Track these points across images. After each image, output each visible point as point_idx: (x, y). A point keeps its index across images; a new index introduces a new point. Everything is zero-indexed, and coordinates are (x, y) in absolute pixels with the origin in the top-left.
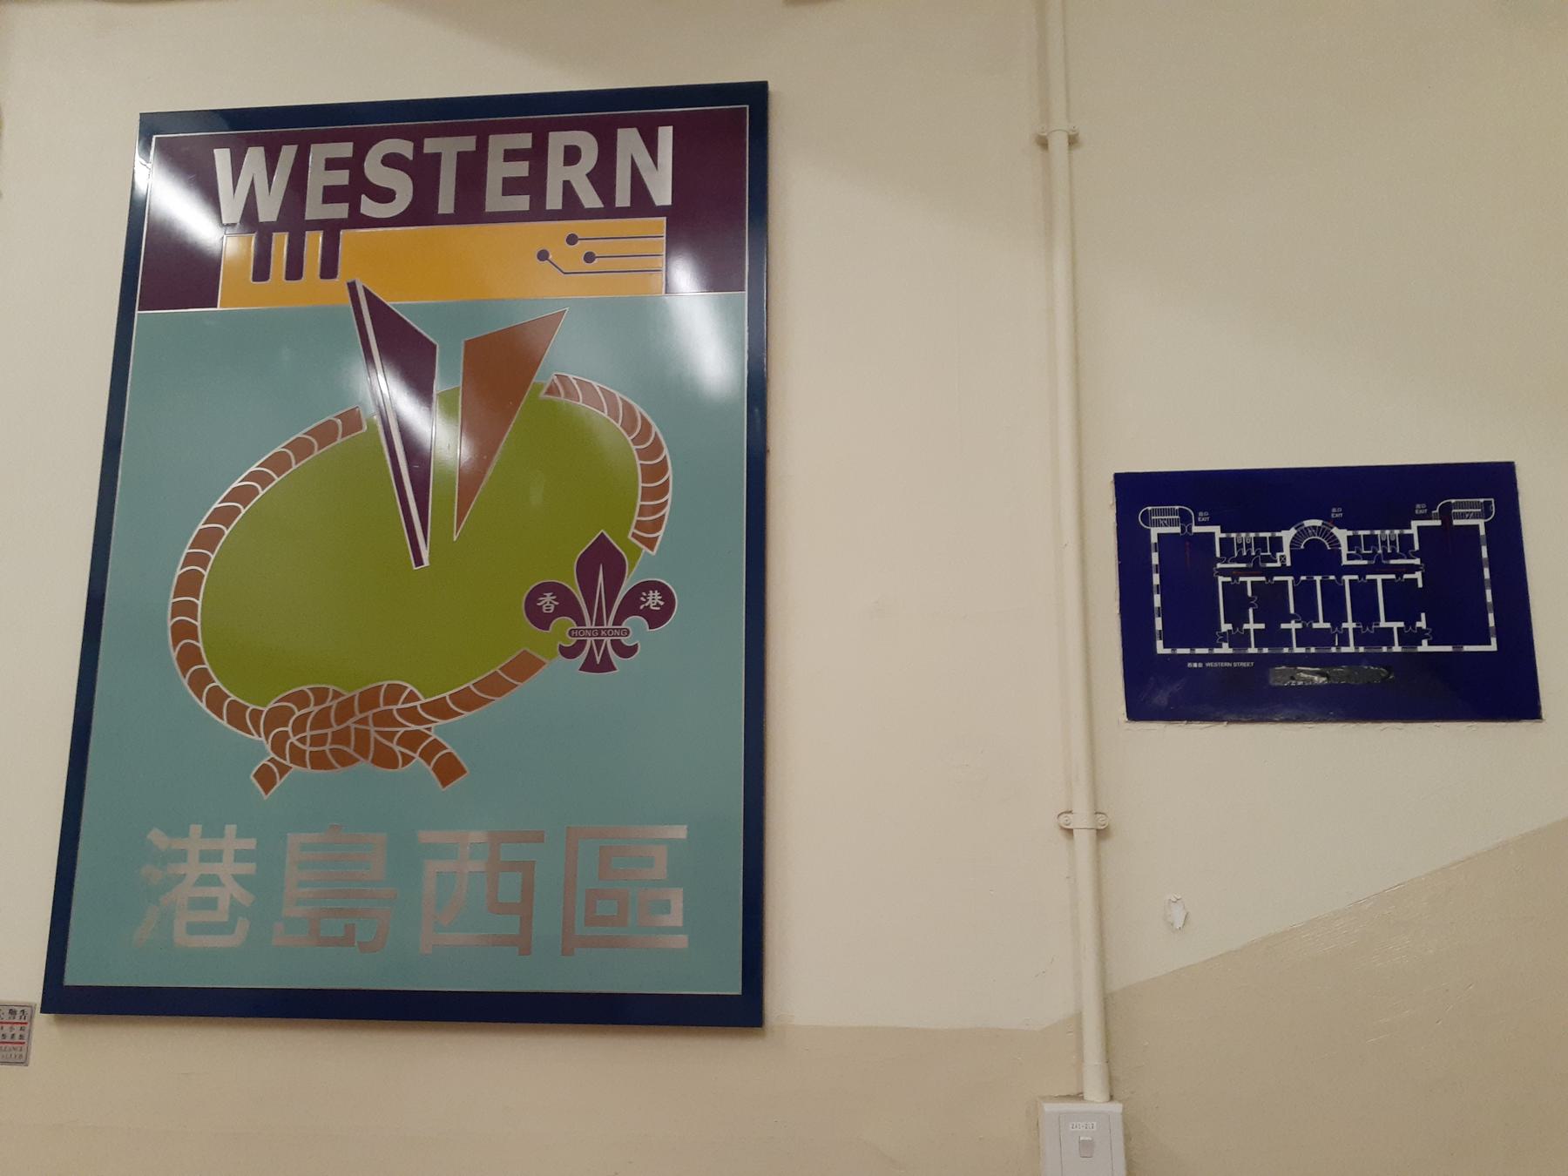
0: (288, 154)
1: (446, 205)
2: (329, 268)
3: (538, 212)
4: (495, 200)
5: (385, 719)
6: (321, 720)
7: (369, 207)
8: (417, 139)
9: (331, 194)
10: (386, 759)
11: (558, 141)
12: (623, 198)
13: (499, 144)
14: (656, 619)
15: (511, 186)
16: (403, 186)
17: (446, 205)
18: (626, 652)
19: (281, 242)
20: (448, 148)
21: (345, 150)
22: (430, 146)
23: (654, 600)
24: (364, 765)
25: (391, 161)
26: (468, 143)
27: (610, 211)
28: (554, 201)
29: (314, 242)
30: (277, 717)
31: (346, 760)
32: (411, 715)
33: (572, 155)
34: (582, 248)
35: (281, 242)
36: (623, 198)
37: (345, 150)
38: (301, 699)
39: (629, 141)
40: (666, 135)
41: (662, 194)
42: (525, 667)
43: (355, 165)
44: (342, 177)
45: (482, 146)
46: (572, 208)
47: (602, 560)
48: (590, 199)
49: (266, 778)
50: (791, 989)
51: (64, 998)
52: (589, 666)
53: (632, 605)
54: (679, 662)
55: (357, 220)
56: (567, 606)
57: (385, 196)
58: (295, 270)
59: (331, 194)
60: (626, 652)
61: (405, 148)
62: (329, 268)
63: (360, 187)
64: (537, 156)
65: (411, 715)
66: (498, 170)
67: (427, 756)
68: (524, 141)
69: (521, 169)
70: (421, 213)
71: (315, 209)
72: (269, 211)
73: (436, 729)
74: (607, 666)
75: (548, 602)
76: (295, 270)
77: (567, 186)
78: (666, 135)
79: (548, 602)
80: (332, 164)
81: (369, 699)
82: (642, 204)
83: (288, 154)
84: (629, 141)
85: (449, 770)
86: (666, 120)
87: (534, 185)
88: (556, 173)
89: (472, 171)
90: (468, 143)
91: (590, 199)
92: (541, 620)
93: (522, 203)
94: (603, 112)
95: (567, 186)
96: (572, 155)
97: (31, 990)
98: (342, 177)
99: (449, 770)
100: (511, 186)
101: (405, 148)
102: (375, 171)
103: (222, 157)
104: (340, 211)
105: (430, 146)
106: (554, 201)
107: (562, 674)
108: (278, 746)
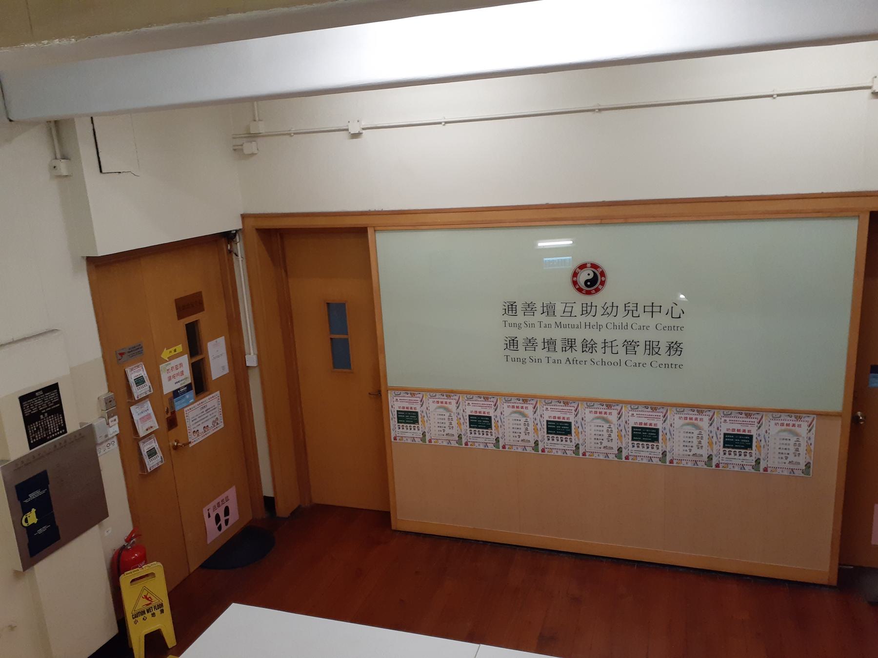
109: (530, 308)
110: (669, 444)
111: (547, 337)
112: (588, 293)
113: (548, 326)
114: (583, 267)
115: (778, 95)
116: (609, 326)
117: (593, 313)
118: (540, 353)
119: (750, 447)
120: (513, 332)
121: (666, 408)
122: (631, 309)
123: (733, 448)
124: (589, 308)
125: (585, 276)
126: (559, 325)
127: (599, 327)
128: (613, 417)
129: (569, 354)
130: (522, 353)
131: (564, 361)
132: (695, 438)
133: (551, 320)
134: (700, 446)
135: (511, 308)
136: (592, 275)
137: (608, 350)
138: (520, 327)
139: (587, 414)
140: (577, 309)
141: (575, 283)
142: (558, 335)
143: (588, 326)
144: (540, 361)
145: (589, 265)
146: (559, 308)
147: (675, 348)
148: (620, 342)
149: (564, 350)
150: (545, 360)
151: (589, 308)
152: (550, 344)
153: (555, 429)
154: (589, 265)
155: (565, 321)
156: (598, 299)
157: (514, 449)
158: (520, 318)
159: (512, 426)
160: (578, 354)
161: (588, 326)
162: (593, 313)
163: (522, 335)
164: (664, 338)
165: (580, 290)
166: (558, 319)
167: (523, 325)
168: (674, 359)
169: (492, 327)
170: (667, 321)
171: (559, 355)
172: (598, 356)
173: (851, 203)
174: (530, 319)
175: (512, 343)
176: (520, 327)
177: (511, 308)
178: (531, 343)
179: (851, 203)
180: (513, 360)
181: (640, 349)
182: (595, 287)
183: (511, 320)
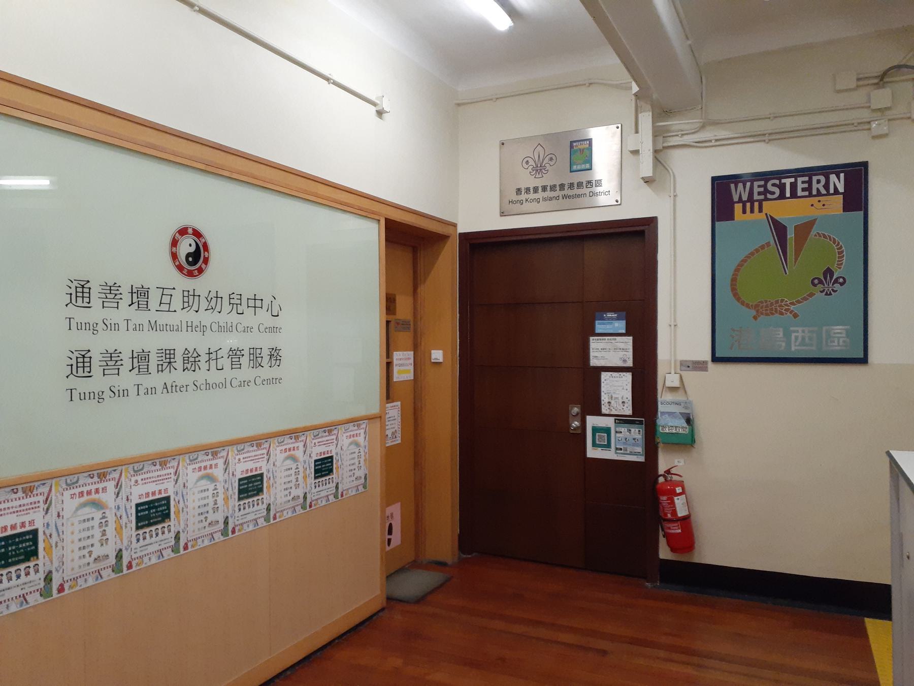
0: (748, 184)
1: (788, 195)
2: (760, 210)
3: (810, 195)
4: (800, 193)
5: (781, 306)
6: (767, 306)
7: (769, 196)
8: (780, 179)
9: (759, 194)
10: (782, 314)
11: (815, 179)
12: (832, 191)
13: (800, 180)
14: (842, 284)
15: (803, 190)
16: (777, 191)
17: (788, 195)
18: (835, 291)
19: (748, 205)
20: (788, 182)
21: (762, 183)
22: (783, 181)
23: (841, 280)
24: (777, 315)
25: (774, 185)
26: (793, 180)
27: (828, 194)
28: (814, 192)
29: (756, 204)
30: (757, 306)
31: (772, 314)
32: (787, 305)
33: (818, 182)
34: (821, 203)
35: (748, 205)
36: (832, 191)
37: (762, 183)
38: (762, 302)
39: (833, 178)
40: (842, 175)
41: (841, 189)
42: (811, 295)
43: (765, 186)
44: (762, 189)
45: (796, 180)
46: (819, 194)
47: (829, 272)
48: (823, 191)
49: (755, 318)
50: (874, 356)
51: (715, 359)
52: (826, 294)
53: (836, 281)
54: (848, 294)
55: (766, 199)
56: (821, 282)
57: (773, 193)
58: (752, 211)
59: (759, 194)
60: (835, 291)
61: (777, 182)
62: (760, 210)
63: (766, 191)
64: (810, 182)
65: (787, 305)
66: (800, 186)
67: (791, 313)
68: (806, 179)
69: (806, 185)
70: (782, 196)
71: (756, 197)
72: (745, 198)
73: (792, 307)
74: (830, 294)
75: (816, 281)
76: (752, 211)
77: (818, 189)
78: (842, 175)
79: (816, 281)
80: (759, 186)
81: (777, 302)
82: (836, 192)
83: (748, 184)
84: (833, 178)
85: (796, 316)
86: (842, 172)
87: (809, 189)
88: (815, 186)
89: (794, 186)
90: (793, 180)
91: (823, 191)
92: (815, 285)
93: (807, 193)
94: (826, 171)
95: (818, 189)
96: (818, 182)
97: (708, 357)
98: (762, 189)
99: (796, 316)
100: (803, 190)
101: (777, 182)
102: (770, 187)
103: (732, 186)
104: (762, 197)
105: (783, 181)
106: (814, 192)
107: (819, 296)
108: (757, 311)
109: (111, 291)
110: (56, 553)
111: (138, 349)
112: (190, 274)
113: (139, 328)
114: (183, 232)
115: (336, 84)
116: (215, 327)
117: (195, 307)
118: (127, 379)
119: (35, 553)
120: (83, 340)
121: (226, 448)
122: (235, 301)
123: (150, 525)
124: (191, 298)
125: (186, 246)
126: (153, 326)
127: (203, 329)
128: (218, 472)
129: (167, 377)
130: (98, 382)
131: (160, 388)
132: (210, 497)
133: (142, 317)
134: (104, 542)
135: (81, 292)
136: (192, 249)
137: (213, 363)
138: (95, 331)
139: (190, 474)
140: (177, 303)
141: (174, 256)
142: (153, 342)
143: (190, 327)
144: (125, 393)
145: (190, 231)
146: (154, 298)
147: (275, 355)
148: (224, 353)
149: (160, 370)
150: (133, 391)
151: (191, 298)
152: (140, 359)
153: (147, 517)
154: (190, 231)
155: (164, 318)
156: (201, 285)
157: (200, 544)
158: (96, 313)
159: (76, 538)
160: (179, 376)
161: (190, 327)
162: (195, 307)
163: (98, 345)
164: (265, 342)
165: (180, 268)
166: (152, 316)
167: (101, 326)
168: (274, 372)
169: (50, 330)
170: (269, 321)
171: (155, 379)
172: (201, 376)
173: (377, 207)
174: (113, 316)
175: (81, 363)
176: (95, 331)
177: (81, 292)
178: (112, 359)
179: (377, 207)
180: (83, 397)
181: (244, 361)
182: (197, 266)
183: (81, 315)
